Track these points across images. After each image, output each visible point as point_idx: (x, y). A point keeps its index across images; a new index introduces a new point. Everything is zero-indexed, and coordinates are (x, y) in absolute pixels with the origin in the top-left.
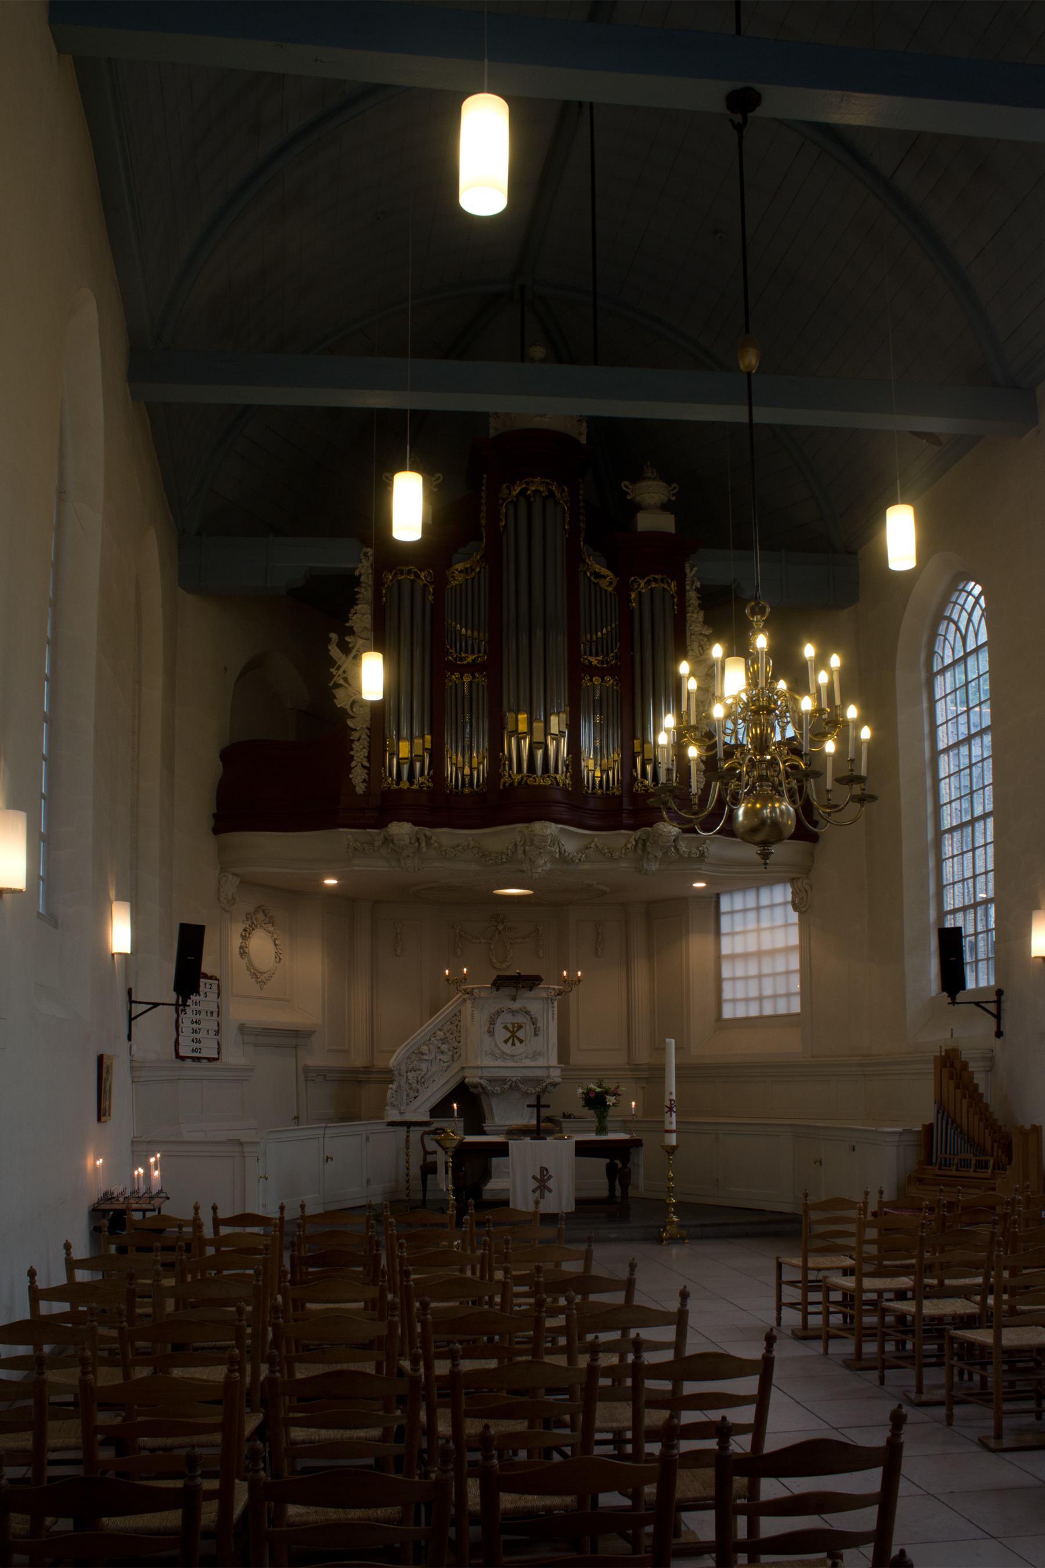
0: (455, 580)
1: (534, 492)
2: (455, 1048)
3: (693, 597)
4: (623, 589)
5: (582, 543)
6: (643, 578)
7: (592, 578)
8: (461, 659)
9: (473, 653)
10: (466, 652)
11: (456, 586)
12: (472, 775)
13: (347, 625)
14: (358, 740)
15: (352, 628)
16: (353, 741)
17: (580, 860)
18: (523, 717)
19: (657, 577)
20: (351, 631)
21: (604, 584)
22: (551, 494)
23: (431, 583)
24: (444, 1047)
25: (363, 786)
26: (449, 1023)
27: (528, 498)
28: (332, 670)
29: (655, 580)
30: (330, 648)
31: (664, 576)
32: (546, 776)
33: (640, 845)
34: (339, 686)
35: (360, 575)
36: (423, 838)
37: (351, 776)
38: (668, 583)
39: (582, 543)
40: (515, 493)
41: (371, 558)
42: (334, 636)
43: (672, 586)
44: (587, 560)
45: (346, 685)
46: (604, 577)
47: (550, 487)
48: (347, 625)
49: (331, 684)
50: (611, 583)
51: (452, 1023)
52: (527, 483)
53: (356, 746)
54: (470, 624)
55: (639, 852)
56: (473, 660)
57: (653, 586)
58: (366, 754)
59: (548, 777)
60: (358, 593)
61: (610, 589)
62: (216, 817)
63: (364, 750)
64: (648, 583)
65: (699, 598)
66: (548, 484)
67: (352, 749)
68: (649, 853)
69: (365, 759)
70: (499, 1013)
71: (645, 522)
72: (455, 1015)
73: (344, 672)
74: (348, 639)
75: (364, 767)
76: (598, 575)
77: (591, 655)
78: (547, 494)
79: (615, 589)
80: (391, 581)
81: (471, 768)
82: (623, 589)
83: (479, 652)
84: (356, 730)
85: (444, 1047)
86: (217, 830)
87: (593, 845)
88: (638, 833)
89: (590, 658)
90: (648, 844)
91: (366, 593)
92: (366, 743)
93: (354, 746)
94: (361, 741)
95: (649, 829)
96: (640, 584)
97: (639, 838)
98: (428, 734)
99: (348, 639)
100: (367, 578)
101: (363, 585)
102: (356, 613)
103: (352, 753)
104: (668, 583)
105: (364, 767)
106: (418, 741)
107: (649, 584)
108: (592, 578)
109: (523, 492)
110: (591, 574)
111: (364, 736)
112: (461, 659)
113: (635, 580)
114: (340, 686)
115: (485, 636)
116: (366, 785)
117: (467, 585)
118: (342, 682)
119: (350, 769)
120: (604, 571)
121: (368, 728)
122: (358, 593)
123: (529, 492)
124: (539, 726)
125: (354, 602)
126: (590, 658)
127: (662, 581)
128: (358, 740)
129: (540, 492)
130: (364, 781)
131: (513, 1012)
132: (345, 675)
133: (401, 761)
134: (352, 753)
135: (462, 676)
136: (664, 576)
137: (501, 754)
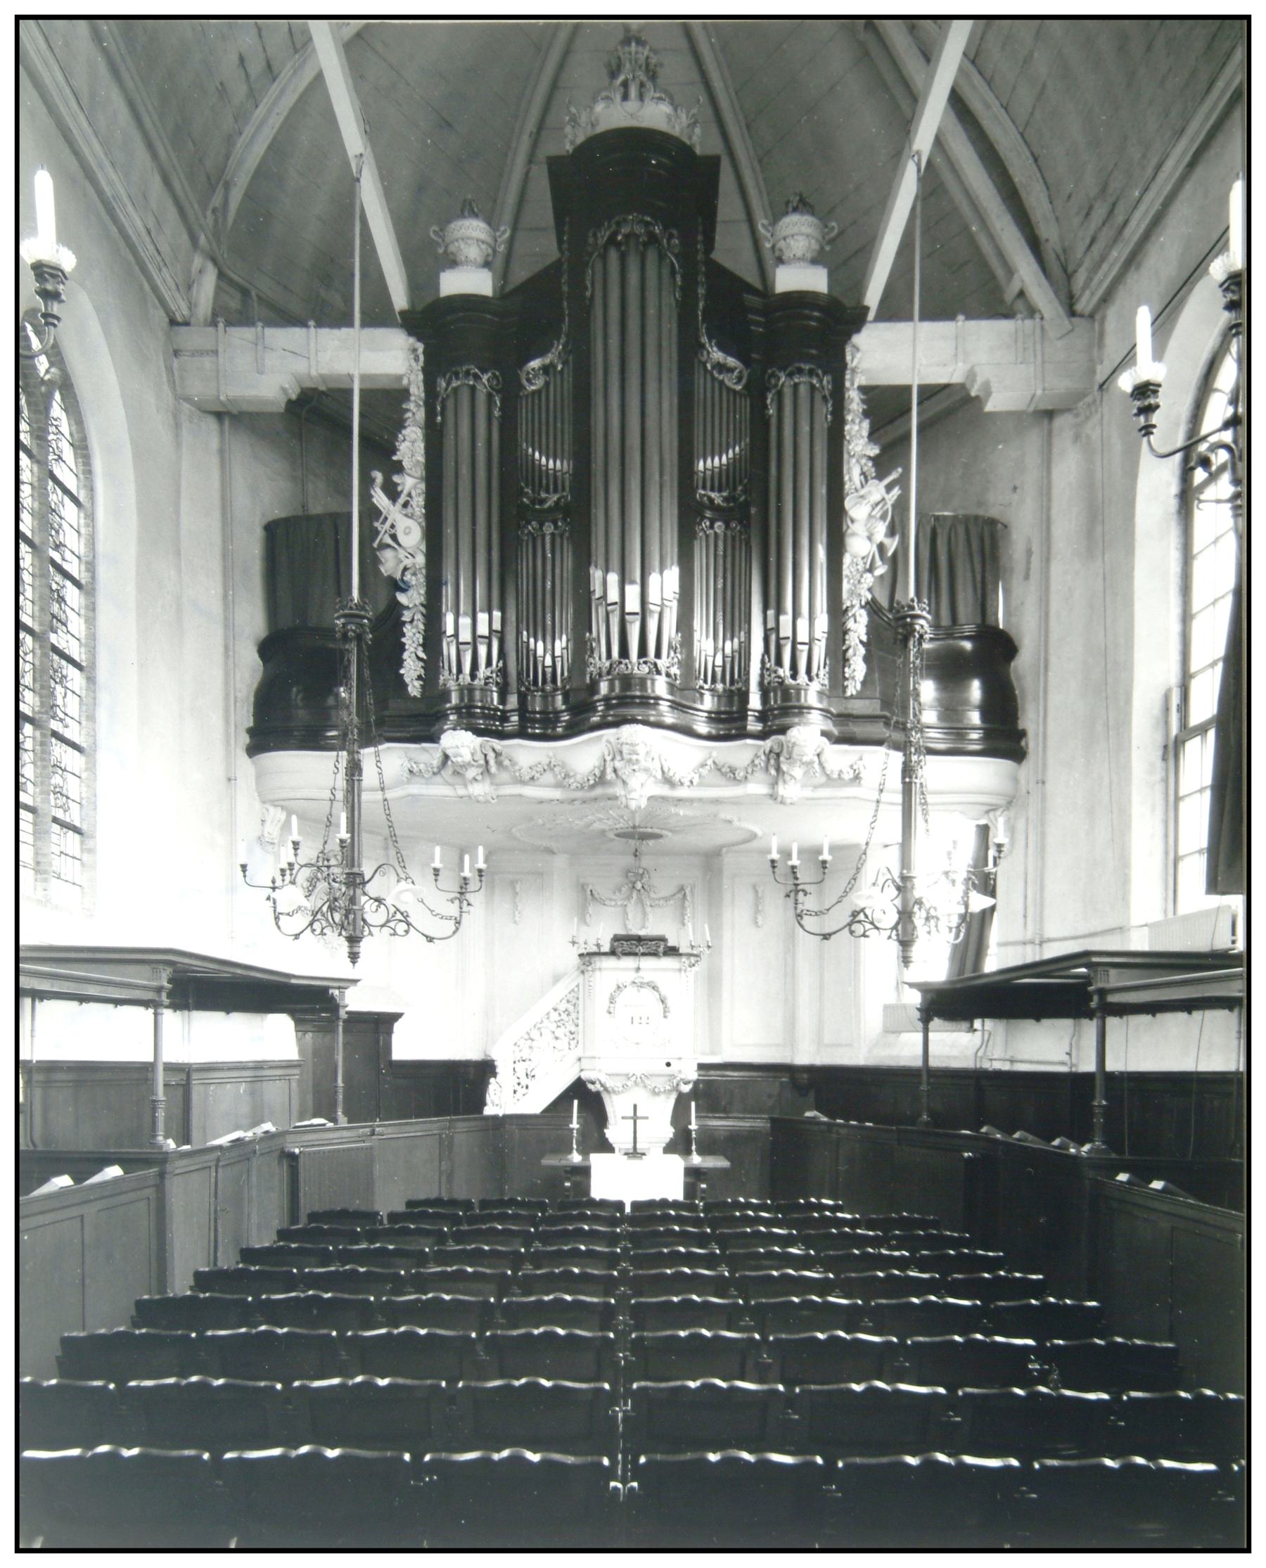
0: (532, 384)
1: (627, 237)
2: (572, 1033)
4: (757, 390)
6: (783, 368)
7: (715, 373)
8: (542, 501)
9: (556, 491)
10: (547, 491)
11: (534, 392)
12: (554, 666)
13: (395, 458)
14: (412, 622)
15: (400, 462)
16: (404, 623)
17: (691, 782)
18: (613, 578)
19: (803, 366)
20: (399, 468)
21: (730, 381)
22: (653, 239)
23: (498, 392)
24: (559, 1033)
25: (418, 684)
26: (564, 1001)
27: (618, 245)
28: (377, 524)
29: (800, 371)
30: (372, 492)
31: (813, 366)
32: (641, 661)
33: (772, 762)
35: (409, 383)
36: (491, 756)
37: (402, 671)
38: (817, 375)
40: (601, 242)
41: (422, 358)
42: (378, 476)
43: (825, 382)
44: (707, 345)
45: (396, 546)
46: (731, 370)
47: (651, 228)
48: (395, 458)
49: (375, 545)
50: (739, 379)
51: (568, 1001)
52: (618, 224)
53: (407, 629)
54: (544, 447)
55: (773, 772)
56: (557, 503)
57: (796, 380)
58: (421, 641)
59: (645, 663)
60: (408, 410)
61: (739, 388)
62: (251, 732)
63: (418, 635)
64: (790, 375)
65: (863, 401)
66: (647, 224)
67: (403, 635)
68: (784, 773)
69: (420, 649)
72: (573, 990)
73: (393, 526)
74: (396, 479)
75: (419, 658)
76: (721, 367)
77: (712, 490)
78: (646, 239)
79: (745, 387)
80: (446, 389)
81: (553, 657)
82: (757, 390)
83: (564, 490)
84: (407, 608)
85: (559, 1033)
86: (255, 749)
87: (710, 762)
88: (768, 744)
89: (713, 495)
90: (782, 759)
91: (415, 412)
92: (422, 627)
93: (405, 630)
94: (415, 623)
95: (781, 737)
96: (779, 379)
97: (771, 751)
98: (482, 611)
99: (396, 479)
100: (417, 390)
101: (412, 398)
102: (405, 440)
103: (404, 640)
104: (817, 375)
105: (419, 658)
106: (483, 618)
107: (792, 379)
108: (715, 373)
109: (612, 240)
110: (713, 367)
111: (418, 616)
112: (542, 501)
113: (773, 373)
114: (389, 546)
115: (569, 465)
116: (421, 683)
117: (548, 391)
118: (389, 541)
119: (400, 663)
120: (731, 361)
121: (422, 605)
122: (408, 410)
123: (619, 238)
124: (633, 592)
125: (400, 425)
126: (713, 495)
127: (811, 373)
128: (412, 622)
129: (637, 236)
130: (419, 678)
132: (393, 531)
133: (461, 647)
134: (404, 640)
135: (541, 525)
136: (813, 366)
137: (588, 634)
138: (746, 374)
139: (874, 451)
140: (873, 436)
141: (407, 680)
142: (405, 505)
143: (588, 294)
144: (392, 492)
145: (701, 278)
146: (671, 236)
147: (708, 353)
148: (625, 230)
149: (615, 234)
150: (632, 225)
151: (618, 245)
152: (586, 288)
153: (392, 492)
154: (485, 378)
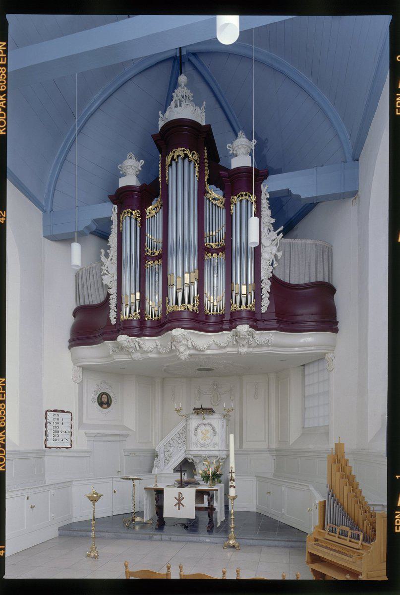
3: (265, 203)
5: (206, 183)
22: (186, 156)
34: (105, 274)
39: (206, 183)
52: (174, 152)
61: (221, 206)
70: (199, 425)
71: (235, 163)
74: (108, 251)
76: (214, 199)
82: (228, 205)
86: (70, 347)
99: (108, 251)
104: (249, 196)
109: (173, 159)
118: (105, 272)
131: (205, 425)
138: (224, 200)
139: (273, 221)
140: (272, 216)
141: (111, 319)
142: (112, 259)
143: (167, 179)
144: (107, 256)
145: (206, 168)
146: (194, 154)
147: (210, 194)
148: (176, 154)
149: (173, 156)
150: (179, 151)
151: (175, 160)
152: (166, 177)
153: (107, 256)
154: (134, 213)
